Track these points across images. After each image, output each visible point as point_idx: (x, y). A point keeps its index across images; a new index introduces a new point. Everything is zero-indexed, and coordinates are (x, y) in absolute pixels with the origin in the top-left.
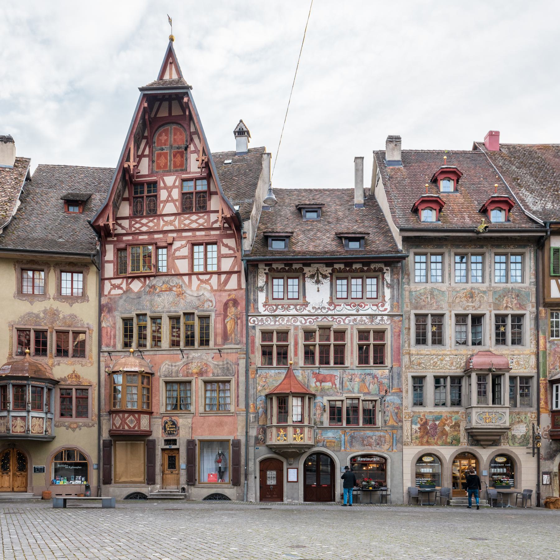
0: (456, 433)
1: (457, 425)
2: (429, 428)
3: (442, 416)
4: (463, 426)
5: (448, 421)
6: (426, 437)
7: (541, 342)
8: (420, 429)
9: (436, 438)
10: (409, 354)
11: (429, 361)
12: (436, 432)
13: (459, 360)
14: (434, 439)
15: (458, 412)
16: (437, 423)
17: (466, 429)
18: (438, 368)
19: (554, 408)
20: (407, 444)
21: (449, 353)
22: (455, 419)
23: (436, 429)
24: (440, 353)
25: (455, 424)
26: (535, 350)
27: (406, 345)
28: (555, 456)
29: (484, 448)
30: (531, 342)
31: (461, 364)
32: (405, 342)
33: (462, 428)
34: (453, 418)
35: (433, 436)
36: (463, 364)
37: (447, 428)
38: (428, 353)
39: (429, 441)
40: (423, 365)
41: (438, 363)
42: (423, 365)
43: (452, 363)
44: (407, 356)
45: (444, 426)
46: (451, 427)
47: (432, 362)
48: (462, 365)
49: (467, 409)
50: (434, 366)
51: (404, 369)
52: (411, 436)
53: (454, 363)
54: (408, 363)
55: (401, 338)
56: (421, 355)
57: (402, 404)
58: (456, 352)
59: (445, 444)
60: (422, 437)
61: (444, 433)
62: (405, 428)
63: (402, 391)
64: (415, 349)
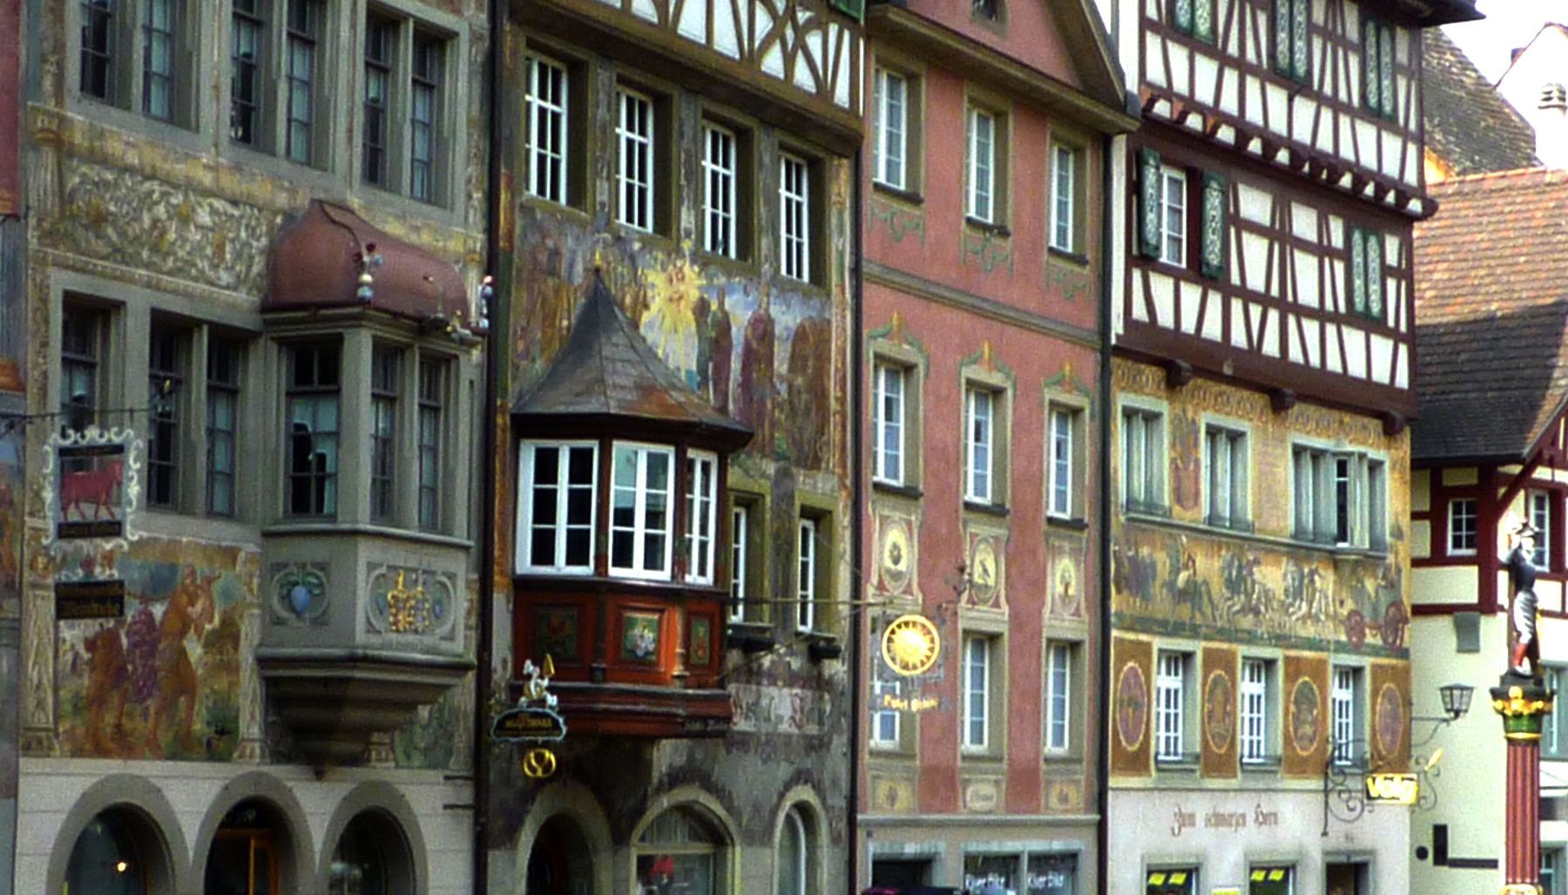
0: (221, 684)
1: (226, 636)
2: (124, 641)
3: (173, 568)
4: (250, 630)
5: (199, 606)
6: (115, 699)
7: (504, 197)
8: (90, 645)
9: (152, 705)
10: (64, 150)
11: (138, 219)
12: (154, 671)
13: (243, 234)
14: (145, 715)
15: (231, 554)
16: (158, 610)
17: (263, 662)
18: (170, 263)
19: (524, 564)
20: (35, 745)
21: (207, 179)
22: (226, 594)
23: (152, 653)
24: (180, 169)
25: (223, 622)
26: (478, 240)
27: (48, 83)
28: (521, 822)
29: (319, 775)
30: (469, 197)
31: (251, 258)
32: (44, 60)
33: (246, 656)
34: (217, 587)
35: (141, 695)
36: (258, 266)
37: (195, 650)
38: (132, 158)
39: (127, 724)
40: (110, 231)
41: (172, 236)
42: (110, 231)
43: (220, 249)
44: (49, 156)
45: (183, 633)
46: (208, 645)
47: (147, 220)
48: (255, 269)
49: (267, 535)
50: (155, 249)
51: (33, 243)
52: (56, 691)
53: (228, 248)
54: (51, 203)
55: (23, 29)
56: (105, 161)
57: (21, 472)
58: (230, 182)
59: (183, 748)
60: (97, 701)
61: (183, 681)
62: (32, 639)
63: (21, 387)
64: (80, 115)
